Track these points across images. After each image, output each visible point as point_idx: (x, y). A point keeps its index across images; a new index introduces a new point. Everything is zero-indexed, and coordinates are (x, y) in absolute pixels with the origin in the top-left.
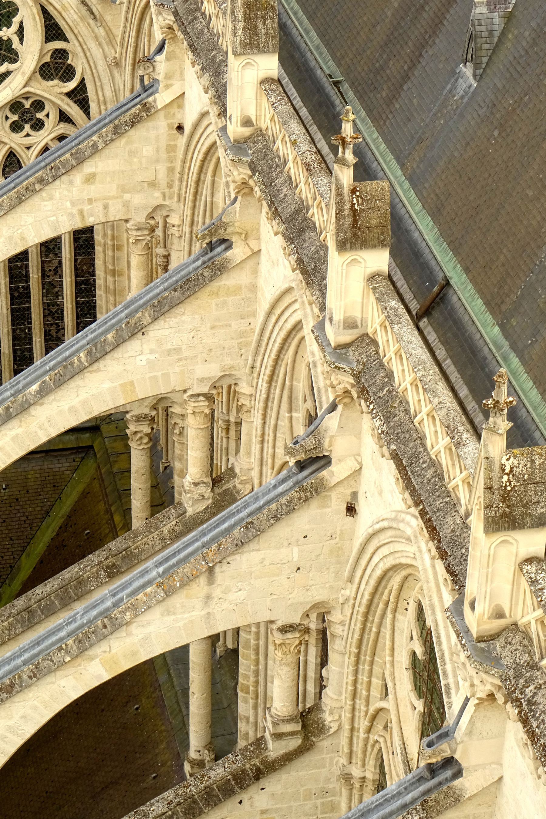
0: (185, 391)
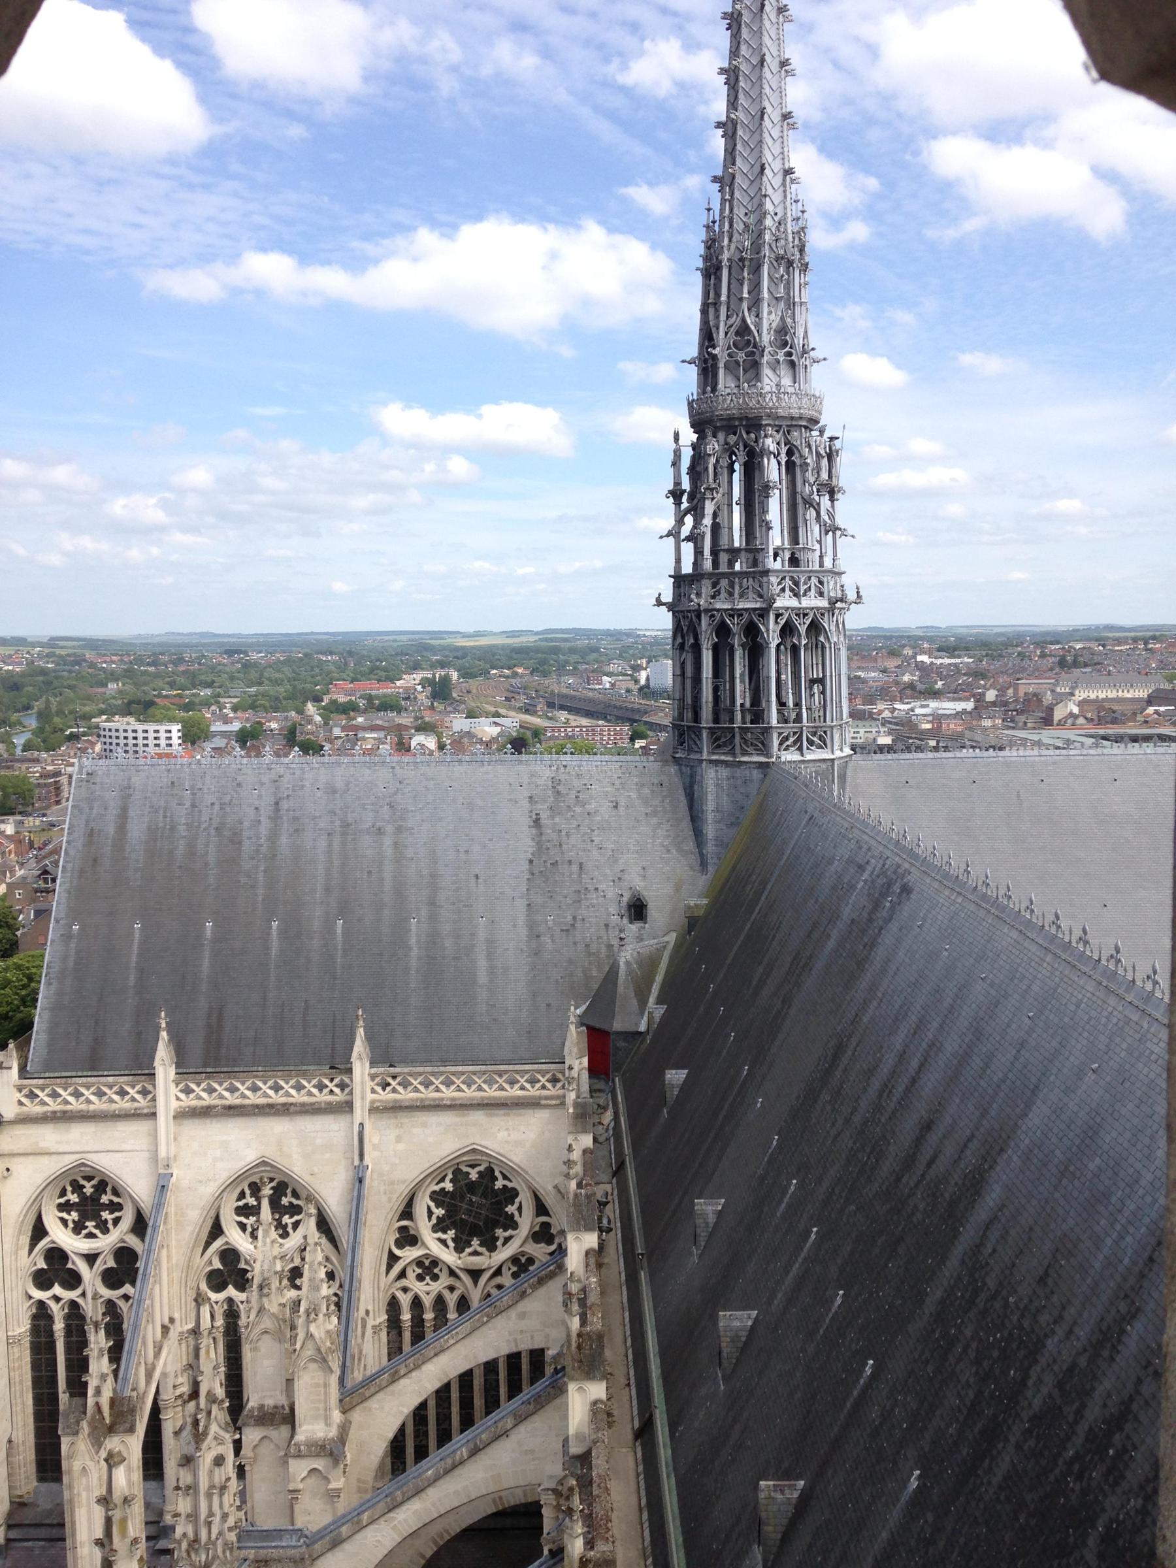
0: (539, 1485)
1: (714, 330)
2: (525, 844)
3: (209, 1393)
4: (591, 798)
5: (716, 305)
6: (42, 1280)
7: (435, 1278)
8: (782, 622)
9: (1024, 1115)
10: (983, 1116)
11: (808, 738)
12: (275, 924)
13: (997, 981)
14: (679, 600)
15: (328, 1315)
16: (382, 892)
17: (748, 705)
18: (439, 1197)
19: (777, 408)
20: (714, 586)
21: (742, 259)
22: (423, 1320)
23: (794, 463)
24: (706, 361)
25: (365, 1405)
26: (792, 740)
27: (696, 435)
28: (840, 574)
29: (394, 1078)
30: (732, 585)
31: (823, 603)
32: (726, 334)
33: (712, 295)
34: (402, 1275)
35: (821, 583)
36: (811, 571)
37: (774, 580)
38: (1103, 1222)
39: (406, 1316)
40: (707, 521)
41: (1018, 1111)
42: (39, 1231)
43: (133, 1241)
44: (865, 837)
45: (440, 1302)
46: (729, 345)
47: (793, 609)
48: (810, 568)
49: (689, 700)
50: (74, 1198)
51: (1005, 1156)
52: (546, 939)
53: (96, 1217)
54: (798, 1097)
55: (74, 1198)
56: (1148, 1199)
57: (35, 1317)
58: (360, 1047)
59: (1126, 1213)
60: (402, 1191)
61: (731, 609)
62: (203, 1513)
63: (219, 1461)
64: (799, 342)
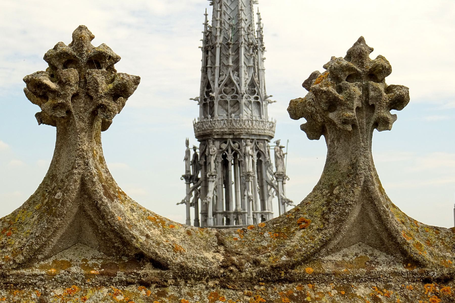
1: (211, 83)
5: (213, 68)
19: (252, 129)
21: (228, 44)
23: (261, 161)
24: (205, 100)
27: (199, 143)
32: (219, 85)
33: (209, 62)
46: (221, 91)
64: (262, 91)
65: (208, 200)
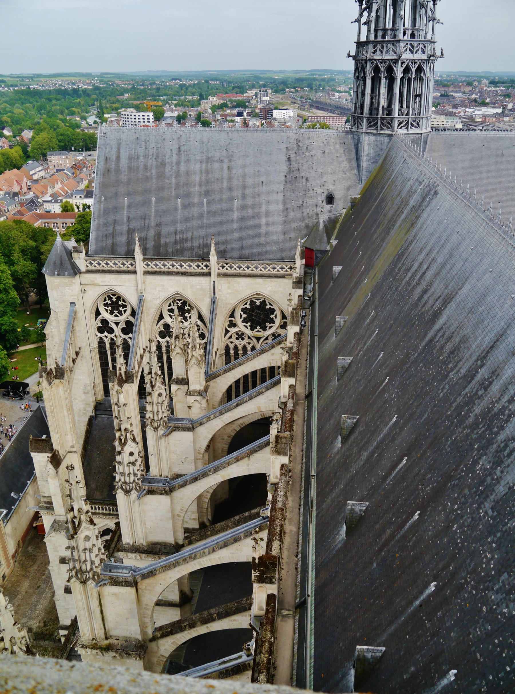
2: (284, 168)
3: (155, 373)
4: (313, 148)
6: (101, 330)
7: (243, 339)
8: (404, 66)
9: (460, 289)
10: (445, 288)
11: (411, 123)
12: (179, 200)
13: (462, 234)
14: (358, 55)
15: (199, 349)
16: (223, 188)
17: (386, 106)
18: (244, 310)
20: (374, 48)
22: (238, 354)
25: (214, 380)
26: (404, 124)
28: (434, 42)
29: (227, 264)
30: (383, 48)
31: (425, 57)
34: (231, 337)
35: (425, 47)
36: (420, 41)
37: (402, 44)
38: (480, 331)
39: (232, 352)
40: (373, 14)
41: (459, 287)
42: (98, 313)
43: (131, 319)
44: (424, 169)
45: (244, 348)
47: (410, 60)
48: (421, 39)
49: (359, 104)
50: (109, 302)
51: (450, 304)
52: (290, 210)
53: (117, 309)
54: (380, 279)
55: (109, 302)
56: (498, 323)
57: (99, 343)
58: (213, 251)
59: (489, 328)
60: (230, 307)
61: (382, 59)
62: (155, 411)
63: (160, 395)
65: (371, 18)
